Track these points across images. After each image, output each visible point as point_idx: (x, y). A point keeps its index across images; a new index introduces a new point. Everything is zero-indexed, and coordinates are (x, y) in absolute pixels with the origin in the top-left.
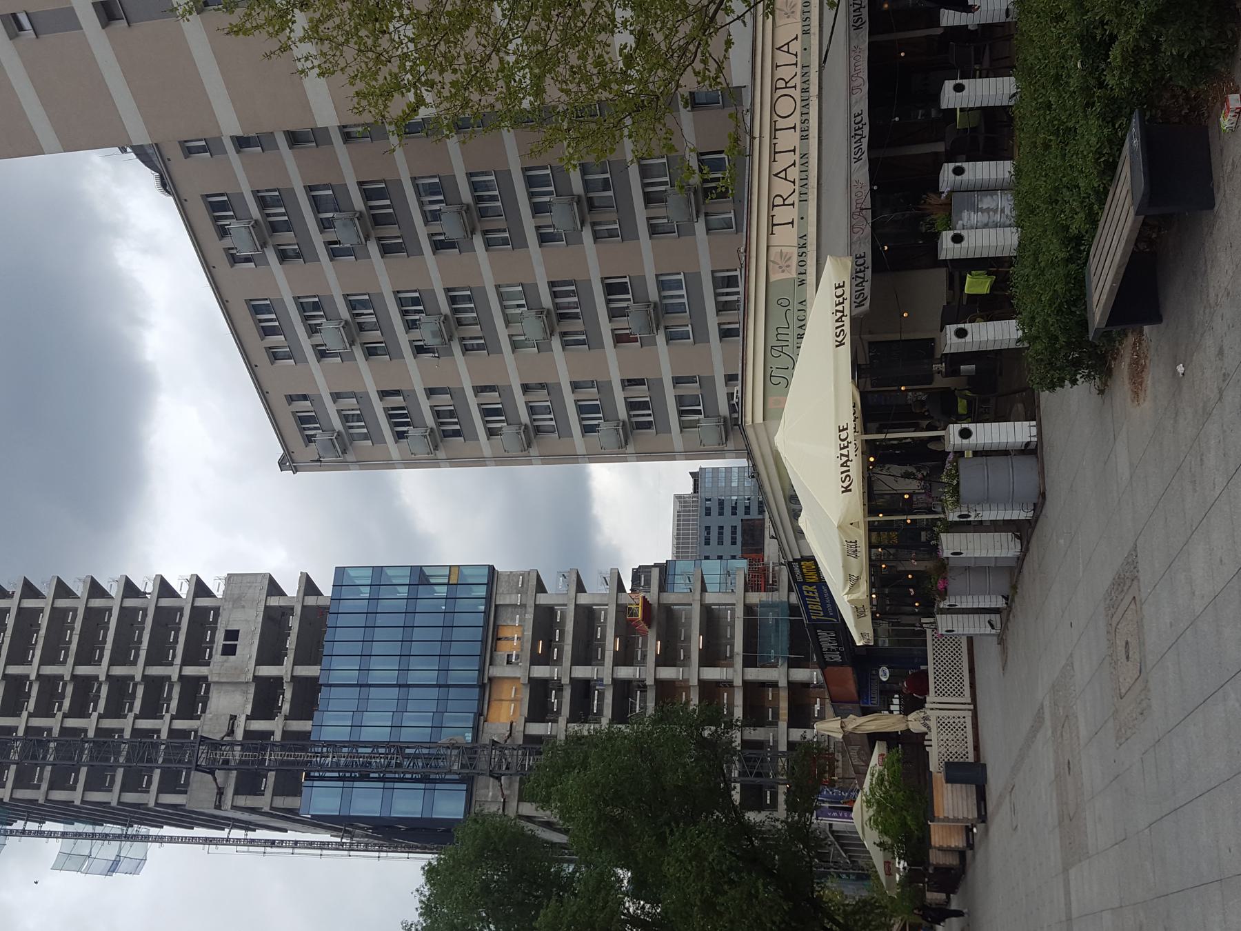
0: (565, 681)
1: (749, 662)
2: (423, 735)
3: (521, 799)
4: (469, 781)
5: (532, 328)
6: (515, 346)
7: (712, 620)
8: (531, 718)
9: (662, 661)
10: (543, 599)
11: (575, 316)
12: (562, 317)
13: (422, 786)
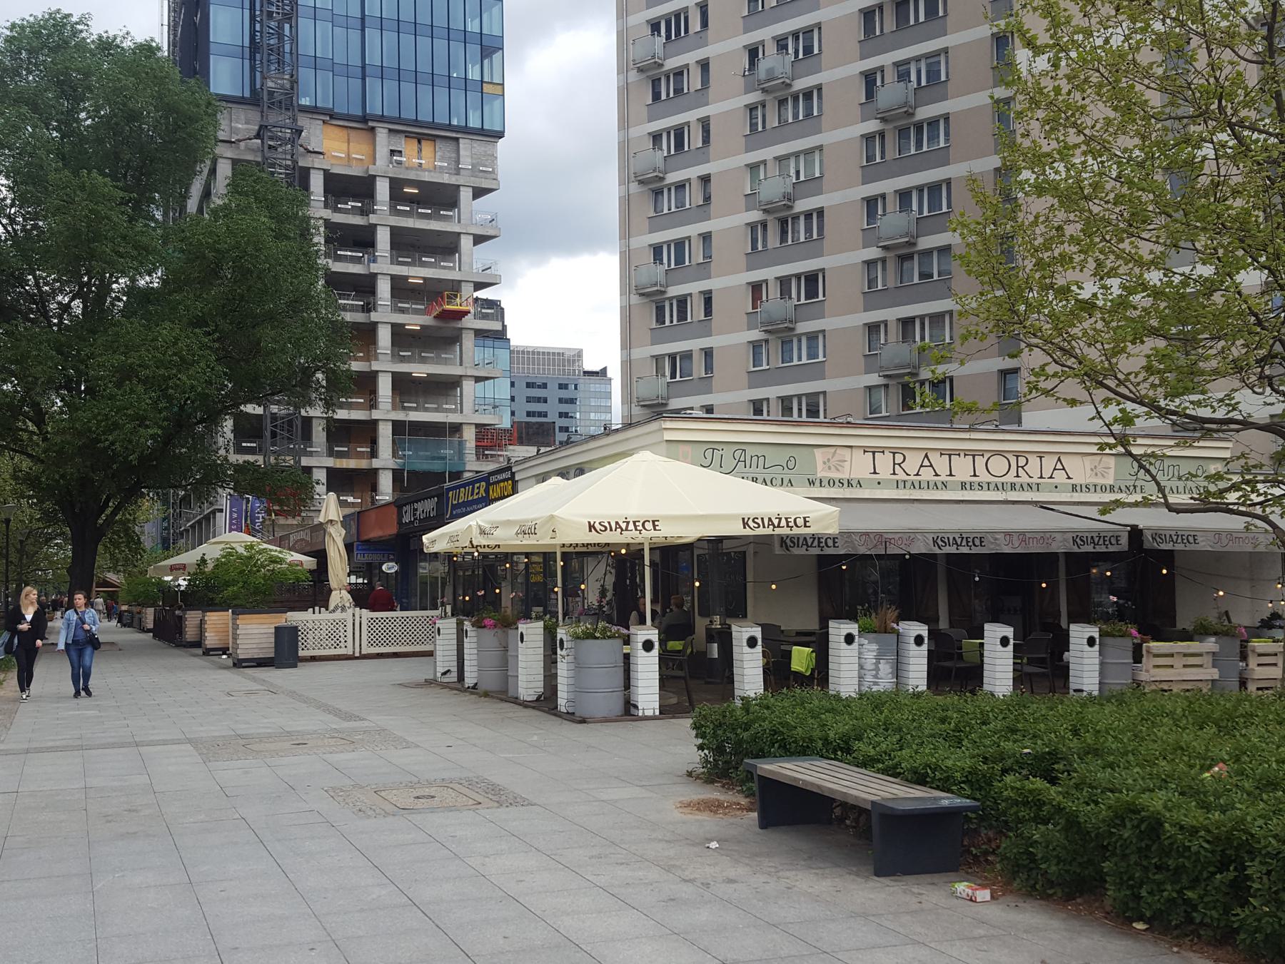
0: (373, 219)
1: (398, 427)
2: (306, 48)
3: (235, 162)
4: (253, 100)
5: (773, 188)
6: (754, 167)
7: (445, 387)
8: (329, 178)
9: (397, 330)
10: (465, 194)
11: (783, 238)
12: (783, 223)
13: (247, 43)
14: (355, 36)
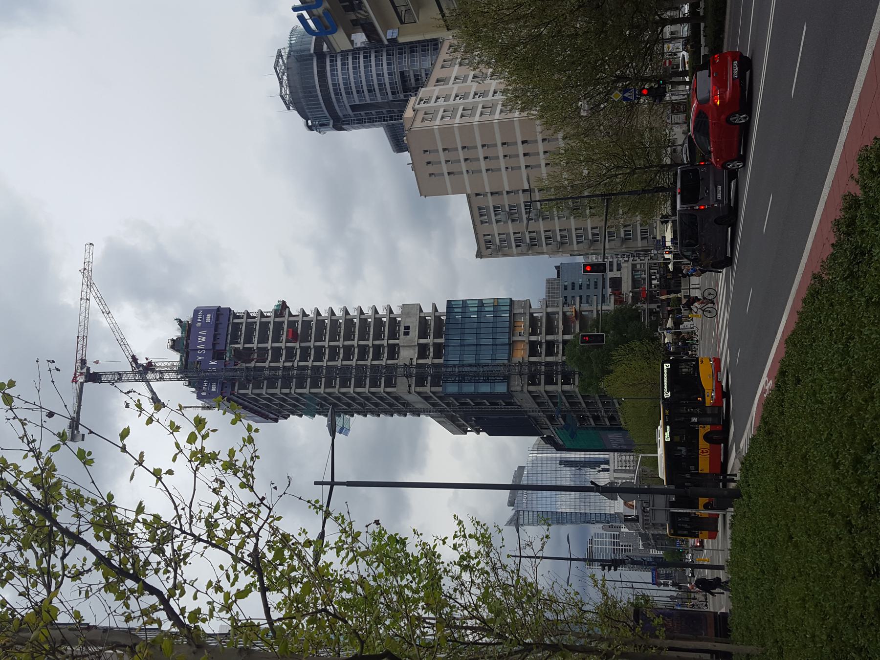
3: (529, 384)
14: (483, 348)
